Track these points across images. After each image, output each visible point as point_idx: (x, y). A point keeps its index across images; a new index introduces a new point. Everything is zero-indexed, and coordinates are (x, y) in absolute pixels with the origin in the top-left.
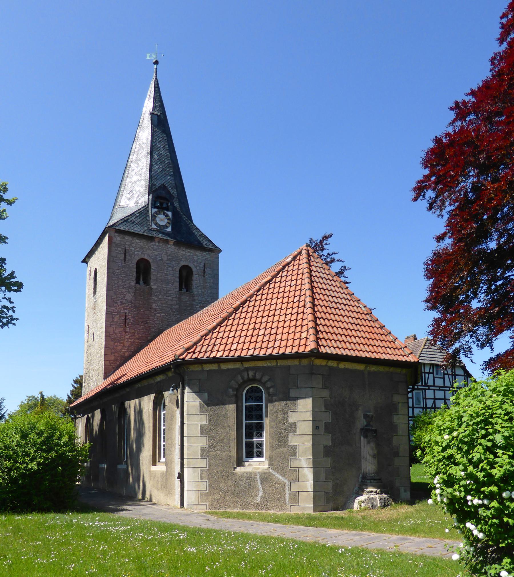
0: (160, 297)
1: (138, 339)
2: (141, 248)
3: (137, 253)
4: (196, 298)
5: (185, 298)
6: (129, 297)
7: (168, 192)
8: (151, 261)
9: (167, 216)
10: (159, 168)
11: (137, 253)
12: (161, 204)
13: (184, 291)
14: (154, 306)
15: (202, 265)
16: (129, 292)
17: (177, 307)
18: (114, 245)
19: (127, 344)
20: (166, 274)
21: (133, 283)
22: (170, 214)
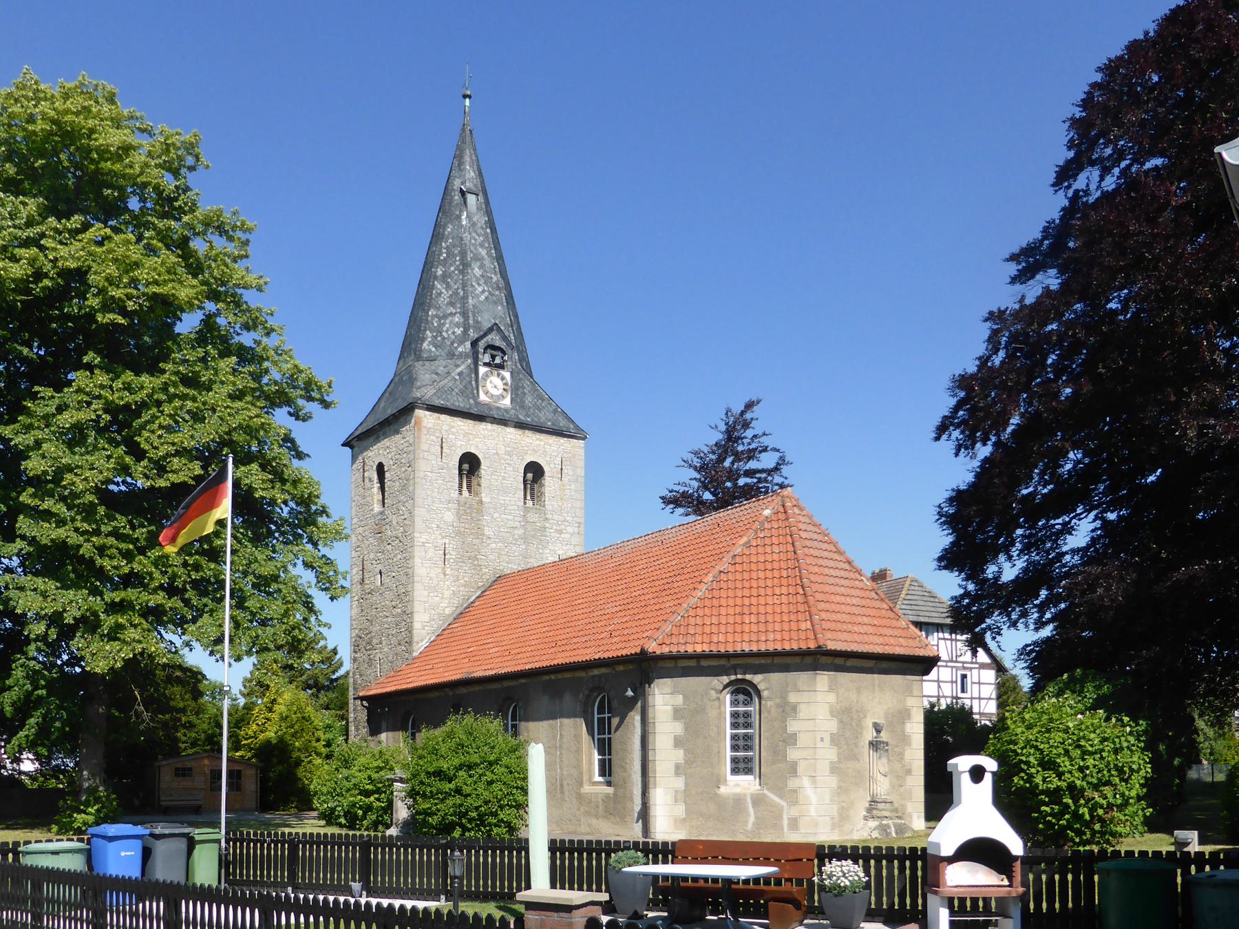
0: (496, 515)
1: (465, 586)
2: (466, 434)
3: (459, 443)
4: (549, 516)
5: (533, 517)
6: (449, 516)
7: (505, 338)
8: (480, 456)
9: (503, 379)
10: (483, 291)
11: (459, 443)
12: (493, 357)
13: (530, 503)
14: (487, 531)
15: (558, 461)
16: (449, 509)
17: (521, 532)
18: (424, 431)
19: (447, 594)
20: (504, 478)
21: (455, 494)
22: (507, 375)
